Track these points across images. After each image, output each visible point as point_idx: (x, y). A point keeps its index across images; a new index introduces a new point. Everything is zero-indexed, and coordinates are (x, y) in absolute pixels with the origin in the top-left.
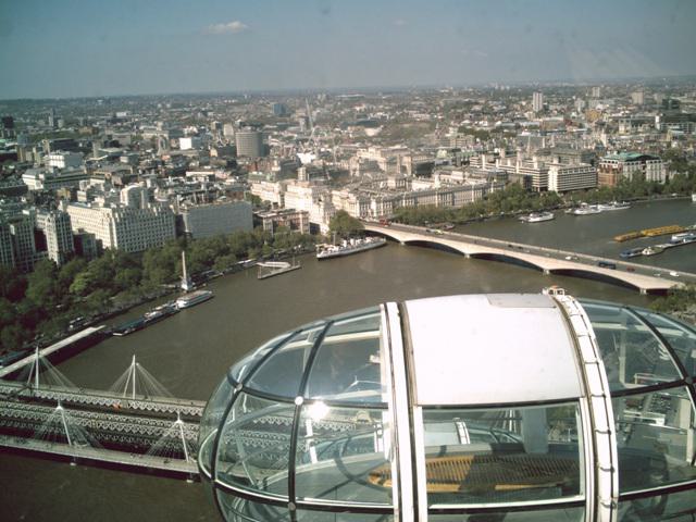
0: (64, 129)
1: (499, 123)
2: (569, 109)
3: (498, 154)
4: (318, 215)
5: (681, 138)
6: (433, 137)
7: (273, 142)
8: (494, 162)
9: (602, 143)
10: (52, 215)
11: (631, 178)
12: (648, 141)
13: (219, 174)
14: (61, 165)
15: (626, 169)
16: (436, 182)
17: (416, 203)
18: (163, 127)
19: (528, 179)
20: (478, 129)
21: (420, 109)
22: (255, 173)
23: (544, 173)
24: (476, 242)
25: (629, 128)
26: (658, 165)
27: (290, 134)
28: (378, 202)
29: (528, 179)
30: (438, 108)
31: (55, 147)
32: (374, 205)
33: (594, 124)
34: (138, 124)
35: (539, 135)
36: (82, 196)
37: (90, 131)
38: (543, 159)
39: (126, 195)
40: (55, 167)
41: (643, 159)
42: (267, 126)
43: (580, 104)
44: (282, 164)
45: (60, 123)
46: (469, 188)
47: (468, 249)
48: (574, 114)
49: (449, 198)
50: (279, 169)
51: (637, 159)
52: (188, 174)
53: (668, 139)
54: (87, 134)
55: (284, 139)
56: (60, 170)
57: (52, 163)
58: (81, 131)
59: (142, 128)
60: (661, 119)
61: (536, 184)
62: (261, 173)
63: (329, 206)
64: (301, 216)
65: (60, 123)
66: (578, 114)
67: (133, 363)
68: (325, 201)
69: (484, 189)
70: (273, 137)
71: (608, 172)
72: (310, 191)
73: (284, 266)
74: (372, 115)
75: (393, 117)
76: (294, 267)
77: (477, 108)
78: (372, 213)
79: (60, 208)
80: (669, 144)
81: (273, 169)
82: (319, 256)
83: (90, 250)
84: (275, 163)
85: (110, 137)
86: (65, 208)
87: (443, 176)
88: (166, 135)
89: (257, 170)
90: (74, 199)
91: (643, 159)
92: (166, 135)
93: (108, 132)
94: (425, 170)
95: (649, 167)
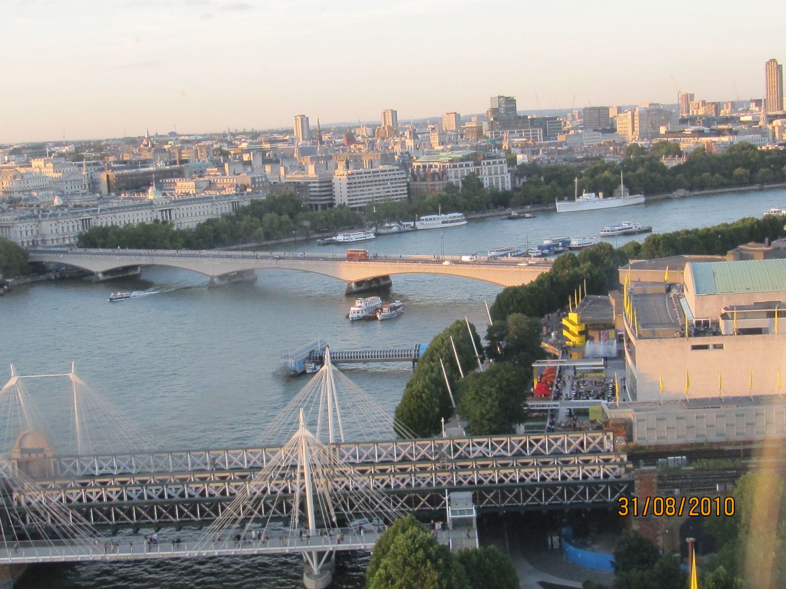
11: (461, 185)
15: (451, 173)
71: (424, 180)
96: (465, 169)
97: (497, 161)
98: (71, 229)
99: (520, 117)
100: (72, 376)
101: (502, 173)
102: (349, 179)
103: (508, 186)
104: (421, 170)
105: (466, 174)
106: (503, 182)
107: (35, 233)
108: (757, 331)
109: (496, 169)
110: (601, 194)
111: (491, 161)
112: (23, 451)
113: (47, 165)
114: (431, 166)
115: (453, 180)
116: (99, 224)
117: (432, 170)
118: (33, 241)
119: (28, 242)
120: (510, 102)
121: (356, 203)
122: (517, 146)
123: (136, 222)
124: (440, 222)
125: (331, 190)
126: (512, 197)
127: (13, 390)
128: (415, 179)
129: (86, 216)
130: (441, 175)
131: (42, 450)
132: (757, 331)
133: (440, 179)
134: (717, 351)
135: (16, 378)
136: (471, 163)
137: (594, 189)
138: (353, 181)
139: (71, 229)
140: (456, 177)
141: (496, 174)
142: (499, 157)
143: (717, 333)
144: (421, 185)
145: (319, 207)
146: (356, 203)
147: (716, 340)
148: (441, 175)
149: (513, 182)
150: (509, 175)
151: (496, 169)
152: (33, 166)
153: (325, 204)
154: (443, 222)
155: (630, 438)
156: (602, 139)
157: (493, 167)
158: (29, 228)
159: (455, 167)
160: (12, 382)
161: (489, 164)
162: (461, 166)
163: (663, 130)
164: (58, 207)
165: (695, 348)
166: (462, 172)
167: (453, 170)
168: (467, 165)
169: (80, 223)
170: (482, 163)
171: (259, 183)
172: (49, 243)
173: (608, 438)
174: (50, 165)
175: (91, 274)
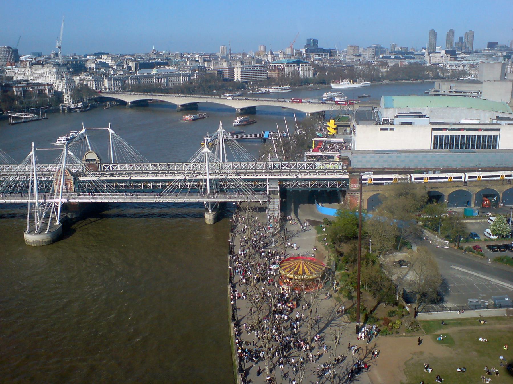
4: (60, 86)
5: (320, 60)
11: (290, 73)
15: (286, 69)
17: (139, 82)
19: (221, 72)
23: (231, 70)
26: (308, 67)
28: (109, 80)
29: (221, 72)
32: (106, 83)
41: (298, 62)
46: (179, 75)
49: (164, 81)
51: (294, 62)
60: (307, 51)
61: (226, 75)
63: (70, 81)
64: (47, 87)
68: (67, 78)
69: (190, 77)
71: (274, 71)
72: (54, 70)
73: (32, 116)
78: (105, 89)
91: (298, 62)
95: (301, 68)
96: (293, 68)
97: (307, 64)
99: (319, 48)
100: (110, 130)
101: (309, 70)
102: (241, 69)
103: (311, 76)
104: (274, 67)
106: (309, 74)
108: (410, 123)
109: (306, 68)
110: (351, 81)
111: (305, 64)
112: (86, 160)
113: (109, 58)
114: (278, 66)
117: (278, 67)
120: (315, 42)
121: (244, 80)
122: (317, 60)
123: (147, 82)
124: (280, 89)
125: (234, 74)
128: (270, 71)
131: (95, 160)
132: (410, 123)
133: (281, 71)
134: (392, 131)
135: (85, 129)
136: (295, 65)
138: (243, 70)
140: (289, 71)
141: (306, 70)
142: (308, 63)
143: (392, 124)
144: (273, 73)
146: (244, 80)
147: (392, 127)
149: (314, 74)
150: (312, 71)
152: (103, 59)
154: (281, 90)
155: (350, 164)
156: (355, 58)
159: (288, 66)
160: (84, 130)
162: (291, 66)
163: (381, 56)
165: (382, 129)
166: (291, 68)
168: (294, 66)
170: (300, 66)
171: (202, 69)
173: (340, 164)
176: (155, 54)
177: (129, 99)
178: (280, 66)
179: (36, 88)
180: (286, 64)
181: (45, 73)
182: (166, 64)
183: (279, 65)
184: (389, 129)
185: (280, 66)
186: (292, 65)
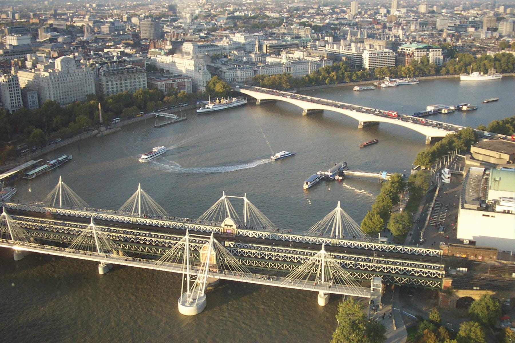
0: (19, 20)
1: (327, 21)
2: (376, 13)
3: (327, 41)
6: (283, 30)
7: (166, 29)
8: (325, 46)
9: (399, 37)
10: (5, 76)
12: (431, 36)
13: (128, 51)
14: (15, 43)
15: (416, 54)
16: (283, 58)
18: (89, 19)
20: (313, 24)
21: (272, 10)
22: (153, 50)
24: (311, 101)
25: (418, 27)
26: (438, 52)
27: (179, 25)
30: (285, 10)
31: (11, 32)
33: (393, 24)
34: (72, 18)
35: (356, 30)
36: (29, 64)
37: (38, 21)
38: (359, 45)
39: (59, 63)
40: (10, 45)
41: (428, 48)
42: (163, 19)
43: (383, 11)
44: (173, 43)
45: (17, 16)
47: (306, 106)
48: (379, 17)
50: (171, 47)
51: (423, 48)
52: (106, 50)
53: (444, 35)
54: (36, 24)
55: (175, 28)
56: (14, 46)
57: (9, 42)
58: (31, 21)
59: (74, 19)
62: (157, 50)
65: (17, 16)
66: (382, 17)
67: (60, 182)
70: (168, 26)
74: (238, 13)
75: (253, 15)
76: (181, 119)
77: (312, 11)
79: (13, 72)
80: (445, 40)
81: (167, 47)
82: (198, 111)
83: (33, 102)
84: (168, 43)
85: (51, 25)
86: (16, 72)
87: (288, 55)
88: (91, 25)
89: (155, 47)
90: (23, 67)
92: (91, 25)
93: (50, 22)
94: (277, 50)
95: (431, 54)
96: (422, 53)
98: (249, 74)
105: (422, 56)
107: (234, 75)
111: (435, 50)
115: (416, 58)
116: (261, 74)
118: (234, 79)
119: (232, 79)
126: (441, 69)
127: (223, 200)
129: (256, 69)
130: (411, 54)
131: (232, 226)
137: (478, 70)
139: (249, 74)
142: (438, 48)
145: (356, 66)
148: (411, 54)
151: (436, 53)
153: (358, 65)
157: (435, 52)
158: (232, 73)
159: (418, 51)
160: (224, 197)
161: (433, 51)
164: (245, 62)
167: (417, 53)
168: (424, 51)
169: (253, 72)
172: (240, 81)
174: (243, 37)
175: (255, 99)
176: (285, 29)
177: (259, 96)
178: (410, 50)
179: (176, 80)
180: (416, 49)
181: (185, 64)
182: (297, 46)
183: (409, 49)
184: (490, 216)
185: (410, 50)
186: (422, 50)
